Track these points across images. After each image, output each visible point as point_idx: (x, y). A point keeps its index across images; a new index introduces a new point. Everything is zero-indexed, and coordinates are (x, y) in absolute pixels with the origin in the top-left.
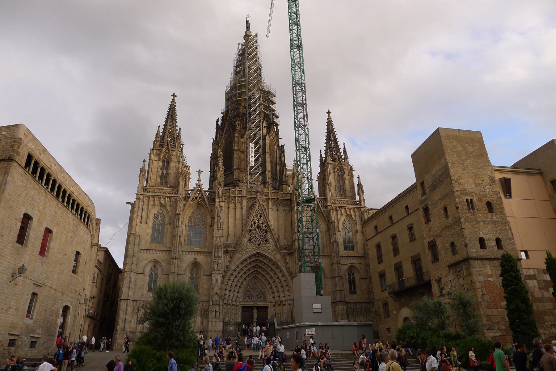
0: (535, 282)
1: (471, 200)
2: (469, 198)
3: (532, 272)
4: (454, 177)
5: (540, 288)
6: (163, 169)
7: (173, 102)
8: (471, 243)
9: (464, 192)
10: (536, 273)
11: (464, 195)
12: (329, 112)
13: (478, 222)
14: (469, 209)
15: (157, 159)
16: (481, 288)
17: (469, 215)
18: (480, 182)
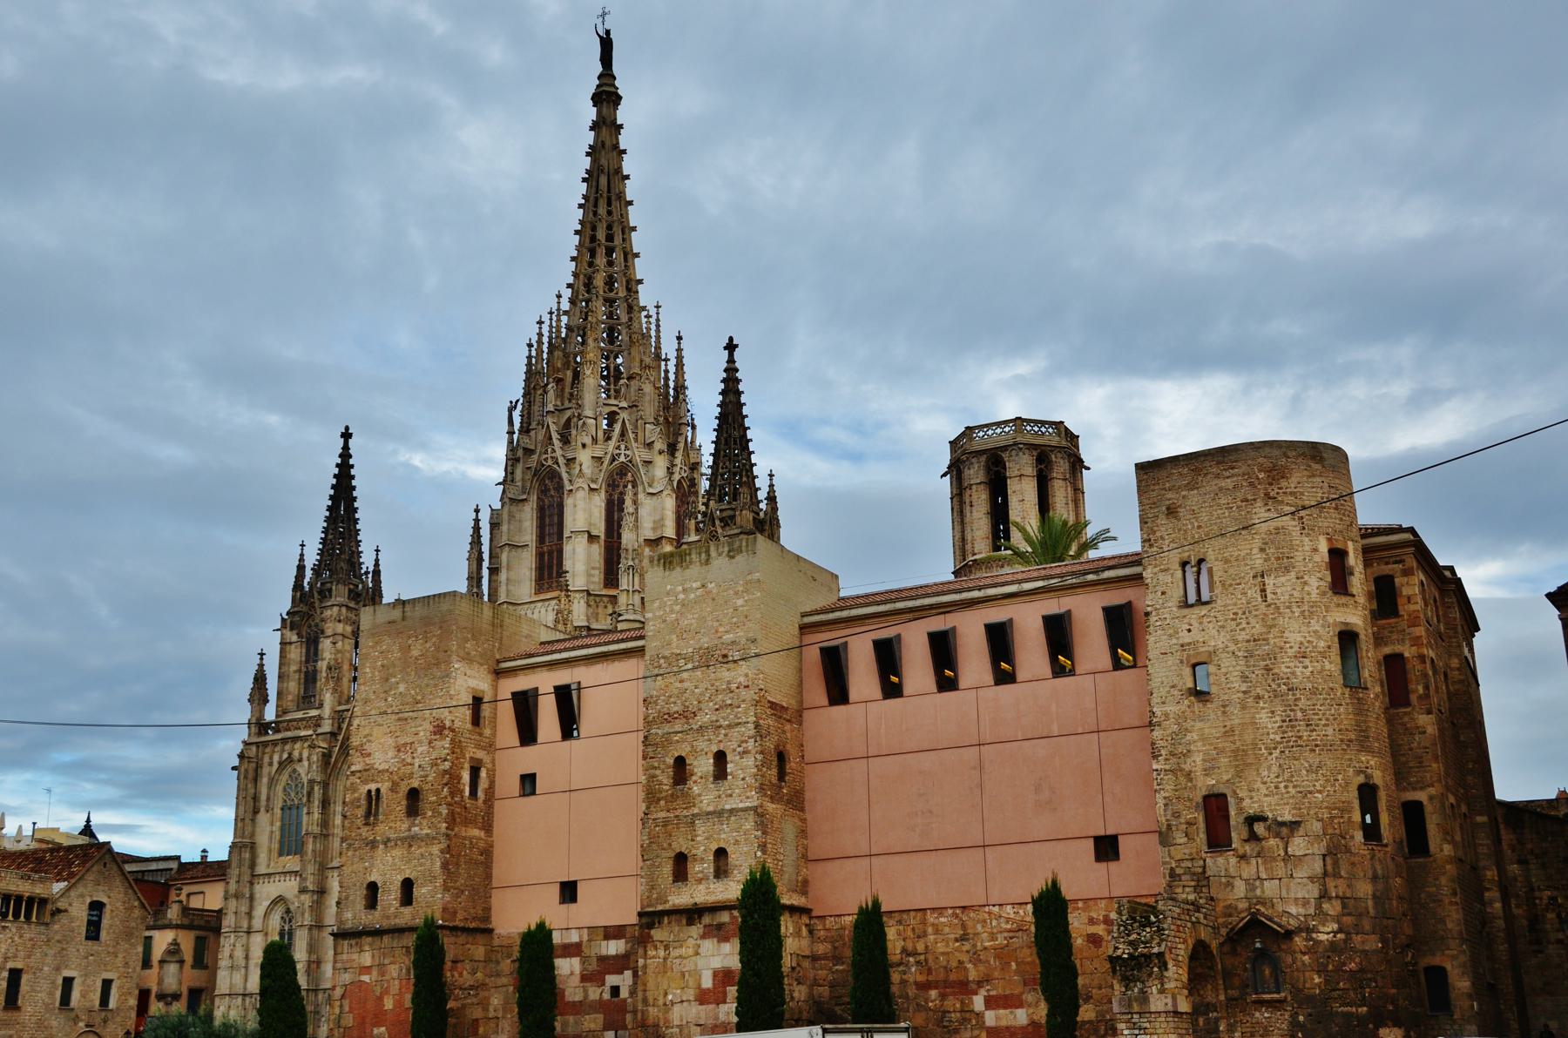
0: (575, 963)
1: (378, 790)
2: (373, 787)
3: (574, 937)
4: (355, 741)
5: (584, 978)
6: (307, 661)
7: (345, 454)
8: (347, 898)
9: (368, 773)
10: (585, 938)
11: (365, 782)
12: (731, 347)
13: (373, 844)
14: (368, 814)
15: (295, 638)
16: (343, 997)
17: (365, 831)
18: (409, 740)
